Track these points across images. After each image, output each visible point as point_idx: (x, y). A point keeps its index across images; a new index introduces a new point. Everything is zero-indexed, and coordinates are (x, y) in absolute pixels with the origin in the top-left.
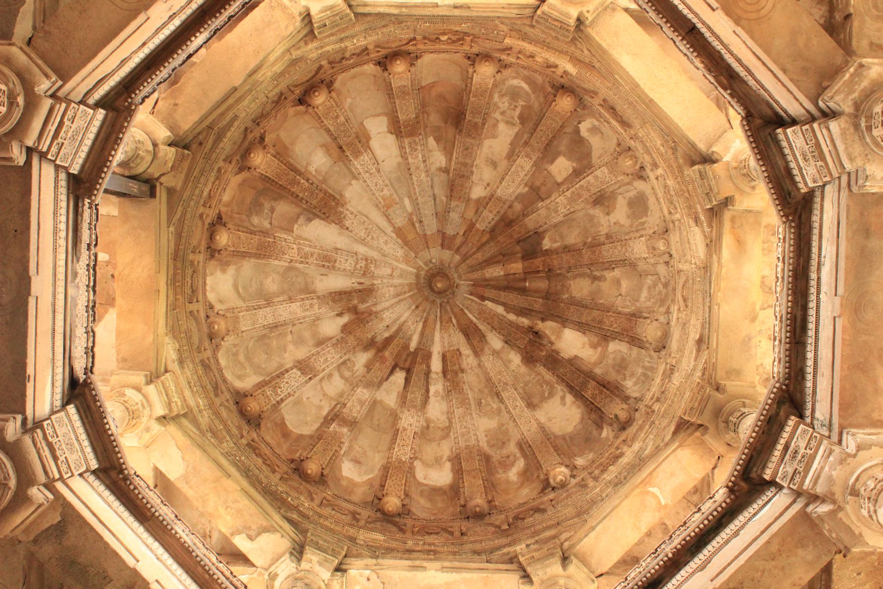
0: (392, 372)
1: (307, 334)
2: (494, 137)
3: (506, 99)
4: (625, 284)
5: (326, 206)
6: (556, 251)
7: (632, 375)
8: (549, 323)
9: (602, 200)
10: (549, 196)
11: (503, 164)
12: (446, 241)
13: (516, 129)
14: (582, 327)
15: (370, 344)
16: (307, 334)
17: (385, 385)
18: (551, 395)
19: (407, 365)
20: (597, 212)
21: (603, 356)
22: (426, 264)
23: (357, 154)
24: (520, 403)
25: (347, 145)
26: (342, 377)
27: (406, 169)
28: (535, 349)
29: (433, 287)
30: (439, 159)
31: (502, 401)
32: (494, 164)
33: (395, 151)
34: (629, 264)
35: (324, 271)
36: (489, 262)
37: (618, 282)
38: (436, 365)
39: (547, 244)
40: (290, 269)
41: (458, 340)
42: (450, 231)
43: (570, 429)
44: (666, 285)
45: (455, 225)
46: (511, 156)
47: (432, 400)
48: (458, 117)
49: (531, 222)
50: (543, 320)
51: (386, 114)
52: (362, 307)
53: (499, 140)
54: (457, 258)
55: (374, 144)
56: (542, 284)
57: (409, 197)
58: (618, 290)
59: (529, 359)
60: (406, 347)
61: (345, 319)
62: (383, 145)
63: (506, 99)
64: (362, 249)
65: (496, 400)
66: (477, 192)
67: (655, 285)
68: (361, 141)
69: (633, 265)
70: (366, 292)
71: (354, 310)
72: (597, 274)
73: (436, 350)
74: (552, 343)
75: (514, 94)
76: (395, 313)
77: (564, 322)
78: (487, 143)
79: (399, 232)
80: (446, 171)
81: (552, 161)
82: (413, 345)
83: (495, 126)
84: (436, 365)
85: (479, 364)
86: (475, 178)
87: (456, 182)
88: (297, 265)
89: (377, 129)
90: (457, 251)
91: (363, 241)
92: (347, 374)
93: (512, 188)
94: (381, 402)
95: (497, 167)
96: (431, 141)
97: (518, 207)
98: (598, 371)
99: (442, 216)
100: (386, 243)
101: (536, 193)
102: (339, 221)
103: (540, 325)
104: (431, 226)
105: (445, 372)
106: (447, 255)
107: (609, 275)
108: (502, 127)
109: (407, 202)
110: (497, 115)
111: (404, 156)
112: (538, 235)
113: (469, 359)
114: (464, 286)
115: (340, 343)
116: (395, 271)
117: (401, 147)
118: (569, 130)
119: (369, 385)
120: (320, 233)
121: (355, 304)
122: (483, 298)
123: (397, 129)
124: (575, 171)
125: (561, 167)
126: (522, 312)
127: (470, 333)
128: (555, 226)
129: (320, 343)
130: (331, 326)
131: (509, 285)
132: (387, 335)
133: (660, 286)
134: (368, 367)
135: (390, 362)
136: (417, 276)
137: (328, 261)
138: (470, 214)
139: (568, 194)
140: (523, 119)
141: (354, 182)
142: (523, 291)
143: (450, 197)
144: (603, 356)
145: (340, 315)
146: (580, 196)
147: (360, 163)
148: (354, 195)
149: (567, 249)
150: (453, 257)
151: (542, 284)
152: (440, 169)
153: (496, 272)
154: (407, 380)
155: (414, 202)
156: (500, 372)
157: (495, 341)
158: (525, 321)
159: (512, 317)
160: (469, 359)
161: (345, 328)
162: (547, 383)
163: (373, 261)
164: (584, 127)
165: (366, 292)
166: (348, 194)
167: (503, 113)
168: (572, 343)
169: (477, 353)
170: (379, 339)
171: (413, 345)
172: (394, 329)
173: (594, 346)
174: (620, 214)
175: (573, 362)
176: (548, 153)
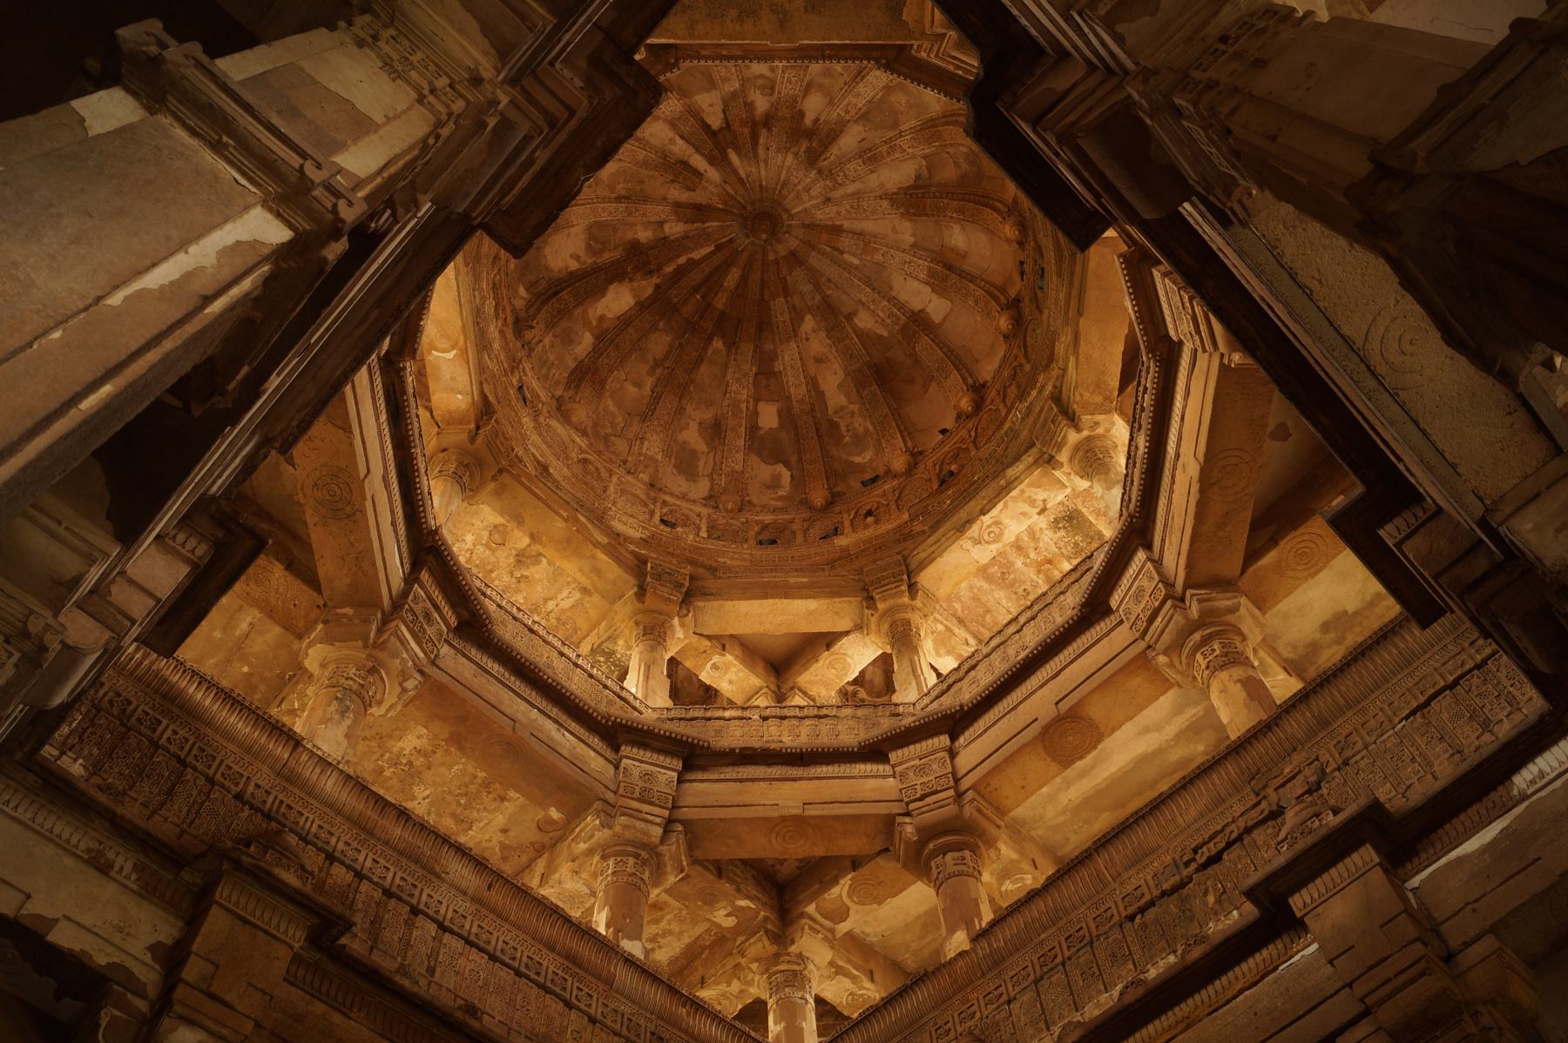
0: (726, 118)
1: (826, 82)
2: (840, 385)
3: (861, 430)
4: (632, 390)
5: (915, 200)
6: (705, 348)
7: (552, 346)
8: (650, 290)
9: (715, 432)
10: (755, 385)
11: (812, 371)
12: (795, 259)
13: (830, 411)
14: (625, 321)
15: (768, 121)
16: (826, 82)
17: (720, 106)
18: (589, 247)
19: (720, 136)
20: (708, 415)
21: (587, 324)
22: (790, 226)
23: (930, 271)
24: (605, 217)
25: (948, 271)
26: (761, 76)
27: (882, 290)
28: (637, 260)
29: (764, 215)
30: (864, 321)
31: (619, 199)
32: (819, 360)
33: (904, 296)
34: (646, 414)
35: (866, 145)
36: (744, 279)
37: (638, 385)
38: (699, 162)
39: (718, 344)
40: (896, 124)
41: (700, 197)
42: (799, 273)
43: (548, 251)
44: (606, 438)
45: (797, 278)
46: (813, 384)
47: (671, 134)
48: (885, 376)
49: (747, 349)
50: (657, 287)
51: (940, 325)
52: (804, 144)
53: (833, 381)
54: (771, 257)
55: (928, 289)
56: (687, 310)
57: (857, 267)
58: (632, 383)
59: (635, 248)
60: (737, 150)
61: (808, 121)
62: (916, 293)
63: (861, 430)
64: (851, 189)
65: (623, 193)
66: (809, 323)
67: (613, 424)
68: (938, 284)
69: (644, 418)
70: (812, 159)
71: (810, 134)
72: (658, 371)
73: (713, 174)
74: (631, 280)
75: (859, 441)
76: (775, 164)
77: (642, 306)
78: (841, 375)
79: (836, 230)
80: (850, 317)
81: (779, 413)
82: (734, 157)
83: (848, 395)
84: (699, 162)
85: (665, 199)
86: (823, 334)
87: (833, 317)
88: (891, 134)
89: (936, 307)
90: (777, 262)
91: (857, 195)
92: (760, 82)
93: (788, 357)
94: (708, 90)
95: (815, 365)
96: (885, 334)
97: (768, 347)
98: (579, 311)
99: (814, 276)
100: (838, 213)
101: (766, 374)
102: (892, 198)
103: (655, 280)
104: (814, 260)
105: (685, 164)
106: (782, 251)
107: (649, 382)
108: (842, 400)
109: (856, 261)
110: (854, 407)
111: (893, 300)
112: (731, 345)
113: (677, 194)
114: (744, 242)
115: (793, 102)
116: (808, 198)
117: (902, 307)
118: (793, 459)
119: (734, 95)
120: (897, 174)
121: (813, 141)
122: (719, 248)
123: (918, 322)
124: (758, 428)
125: (769, 417)
126: (680, 272)
127: (699, 212)
128: (726, 366)
129: (809, 86)
130: (813, 106)
131: (711, 282)
132: (762, 140)
133: (609, 431)
134: (750, 106)
135: (736, 126)
136: (787, 211)
137: (870, 157)
138: (796, 300)
139: (743, 406)
140: (834, 426)
141: (912, 240)
142: (695, 290)
143: (825, 299)
144: (587, 324)
145: (817, 120)
146: (734, 415)
147: (922, 266)
148: (906, 232)
149: (699, 361)
150: (776, 253)
151: (687, 310)
152: (855, 313)
153: (732, 278)
154: (706, 127)
155: (848, 267)
156: (644, 215)
157: (674, 229)
158: (669, 269)
159: (682, 260)
160: (677, 194)
161: (802, 114)
162: (601, 251)
163: (834, 188)
164: (786, 474)
165: (812, 159)
166: (908, 224)
167: (853, 413)
168: (618, 301)
169: (677, 205)
170: (764, 133)
171: (734, 157)
172: (761, 151)
173: (602, 318)
174: (692, 436)
175: (601, 291)
176: (786, 416)
